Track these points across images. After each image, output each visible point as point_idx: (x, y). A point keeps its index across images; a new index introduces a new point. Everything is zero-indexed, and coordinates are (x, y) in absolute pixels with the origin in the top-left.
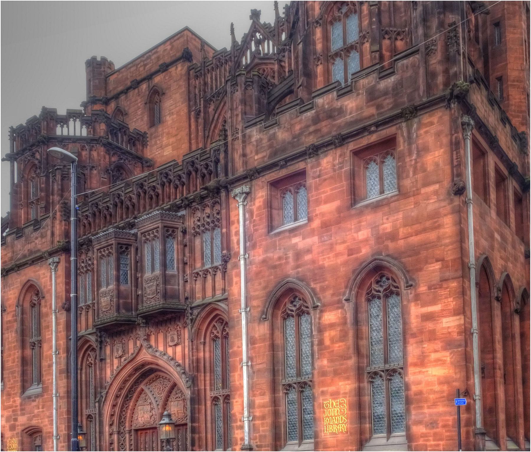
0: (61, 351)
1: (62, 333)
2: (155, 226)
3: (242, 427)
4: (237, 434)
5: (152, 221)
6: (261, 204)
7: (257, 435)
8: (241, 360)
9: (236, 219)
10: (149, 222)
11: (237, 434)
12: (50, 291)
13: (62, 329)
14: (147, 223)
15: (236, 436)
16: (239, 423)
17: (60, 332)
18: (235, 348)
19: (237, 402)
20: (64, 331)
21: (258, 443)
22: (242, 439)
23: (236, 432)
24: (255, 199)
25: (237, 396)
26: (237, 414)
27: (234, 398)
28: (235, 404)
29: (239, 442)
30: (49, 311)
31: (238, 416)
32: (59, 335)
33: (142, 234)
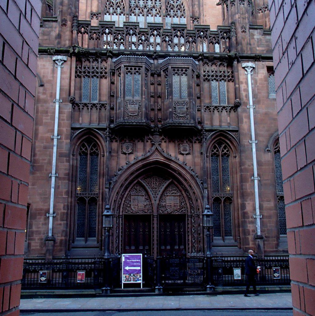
0: (64, 137)
1: (66, 121)
2: (186, 67)
3: (254, 222)
4: (250, 227)
5: (184, 63)
6: (263, 77)
7: (266, 229)
8: (253, 175)
9: (244, 81)
10: (181, 63)
11: (250, 227)
12: (53, 83)
13: (65, 118)
14: (179, 62)
15: (248, 228)
16: (251, 219)
17: (63, 120)
18: (246, 166)
19: (248, 204)
20: (67, 120)
21: (267, 235)
22: (255, 231)
23: (249, 225)
24: (258, 73)
25: (248, 200)
26: (249, 212)
27: (246, 201)
28: (247, 205)
29: (251, 233)
30: (49, 98)
31: (250, 214)
32: (62, 122)
33: (172, 68)
